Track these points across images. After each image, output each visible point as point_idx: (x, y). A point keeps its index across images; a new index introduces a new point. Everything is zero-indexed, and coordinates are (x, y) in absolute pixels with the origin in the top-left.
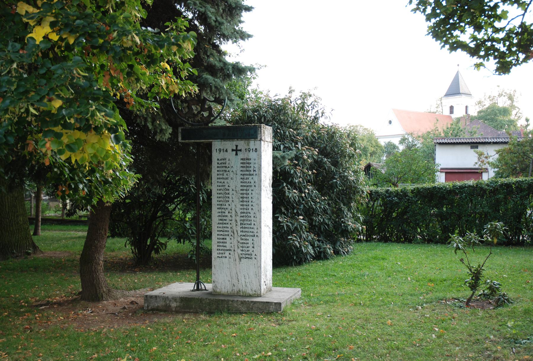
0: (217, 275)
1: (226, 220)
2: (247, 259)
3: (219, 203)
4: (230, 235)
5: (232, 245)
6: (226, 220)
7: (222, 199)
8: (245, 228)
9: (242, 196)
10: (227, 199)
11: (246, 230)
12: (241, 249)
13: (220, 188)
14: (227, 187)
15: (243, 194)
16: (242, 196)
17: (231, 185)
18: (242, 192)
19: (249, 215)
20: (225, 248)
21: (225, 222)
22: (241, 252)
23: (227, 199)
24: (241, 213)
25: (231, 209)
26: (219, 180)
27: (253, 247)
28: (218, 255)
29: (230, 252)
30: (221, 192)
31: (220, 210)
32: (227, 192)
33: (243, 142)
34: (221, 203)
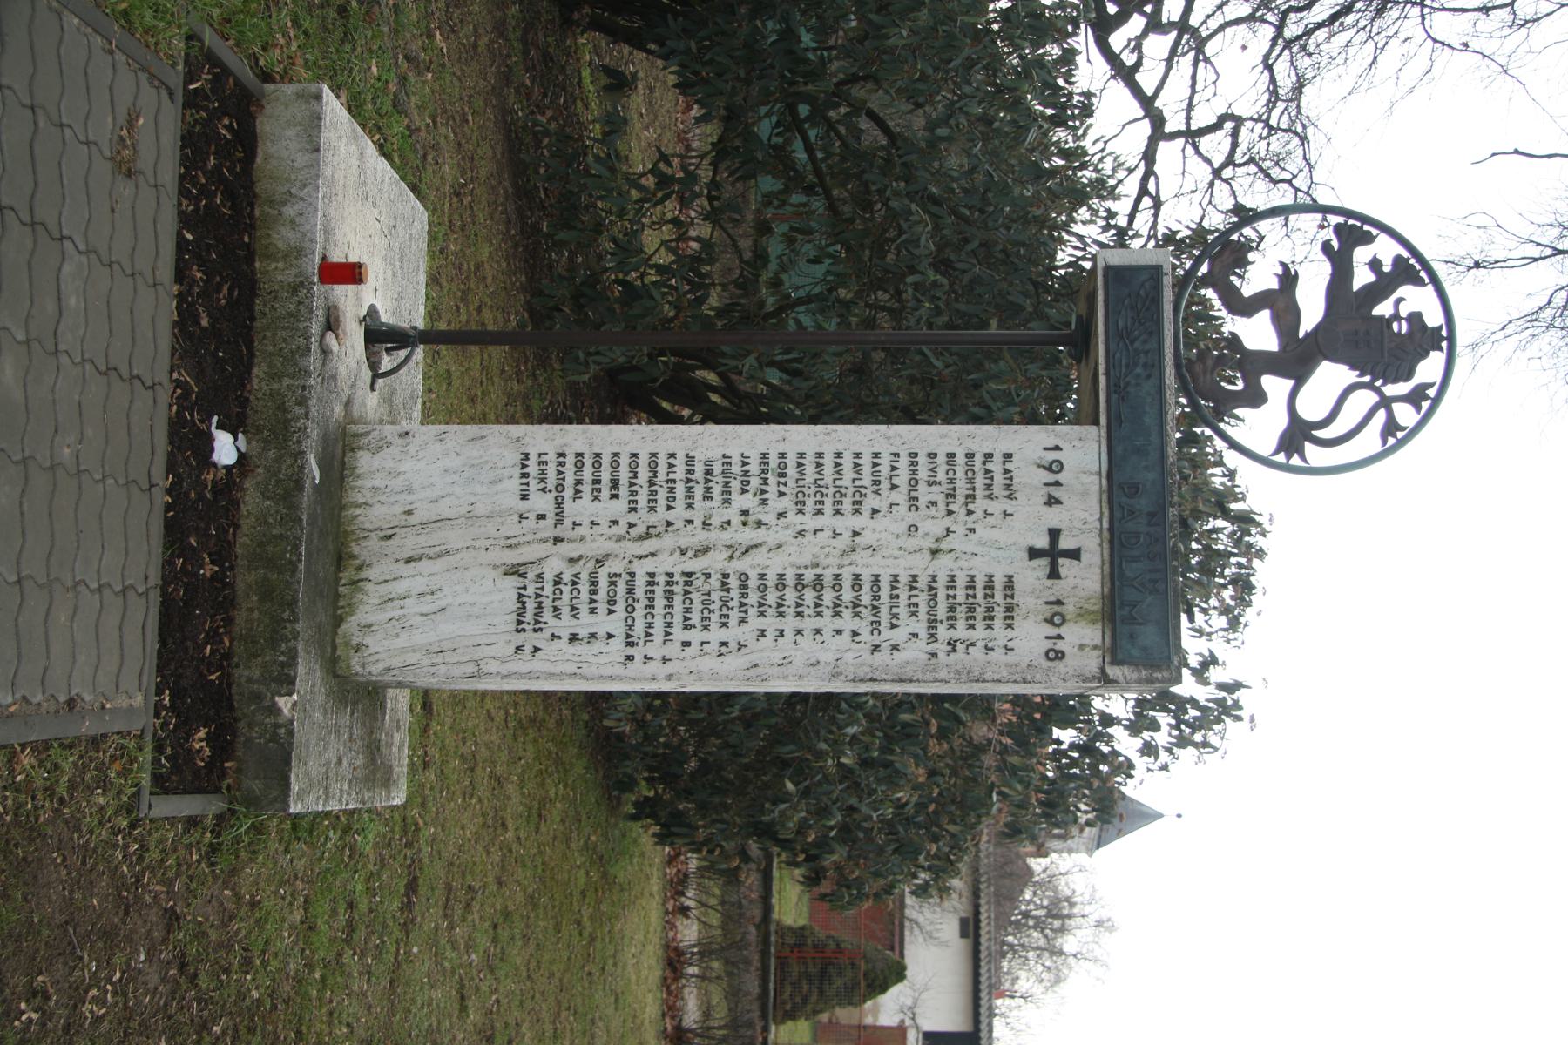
0: (437, 448)
1: (707, 497)
2: (513, 605)
3: (791, 461)
4: (633, 518)
5: (584, 530)
6: (707, 497)
7: (809, 479)
8: (669, 595)
9: (828, 580)
10: (810, 504)
11: (660, 603)
12: (566, 578)
13: (867, 469)
14: (871, 501)
15: (837, 586)
16: (828, 580)
17: (882, 522)
18: (847, 582)
19: (735, 616)
20: (568, 493)
21: (699, 491)
22: (549, 577)
23: (810, 504)
24: (743, 577)
25: (759, 524)
26: (903, 462)
27: (574, 638)
28: (533, 458)
29: (551, 519)
30: (848, 473)
31: (754, 468)
32: (847, 505)
33: (1097, 587)
34: (792, 471)
